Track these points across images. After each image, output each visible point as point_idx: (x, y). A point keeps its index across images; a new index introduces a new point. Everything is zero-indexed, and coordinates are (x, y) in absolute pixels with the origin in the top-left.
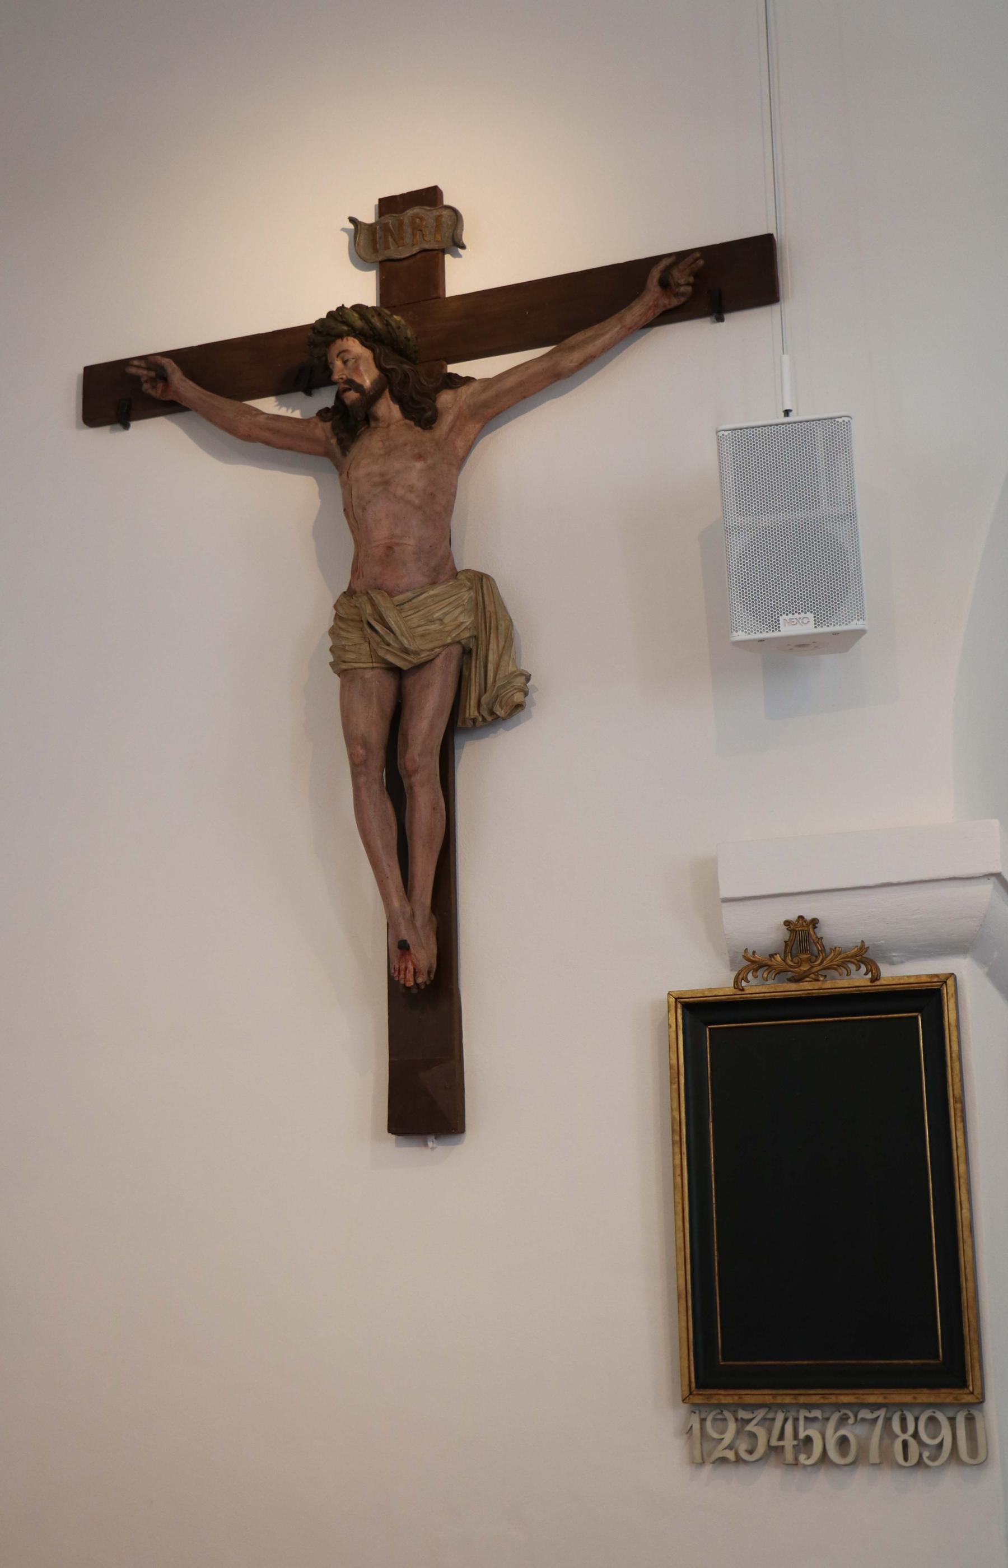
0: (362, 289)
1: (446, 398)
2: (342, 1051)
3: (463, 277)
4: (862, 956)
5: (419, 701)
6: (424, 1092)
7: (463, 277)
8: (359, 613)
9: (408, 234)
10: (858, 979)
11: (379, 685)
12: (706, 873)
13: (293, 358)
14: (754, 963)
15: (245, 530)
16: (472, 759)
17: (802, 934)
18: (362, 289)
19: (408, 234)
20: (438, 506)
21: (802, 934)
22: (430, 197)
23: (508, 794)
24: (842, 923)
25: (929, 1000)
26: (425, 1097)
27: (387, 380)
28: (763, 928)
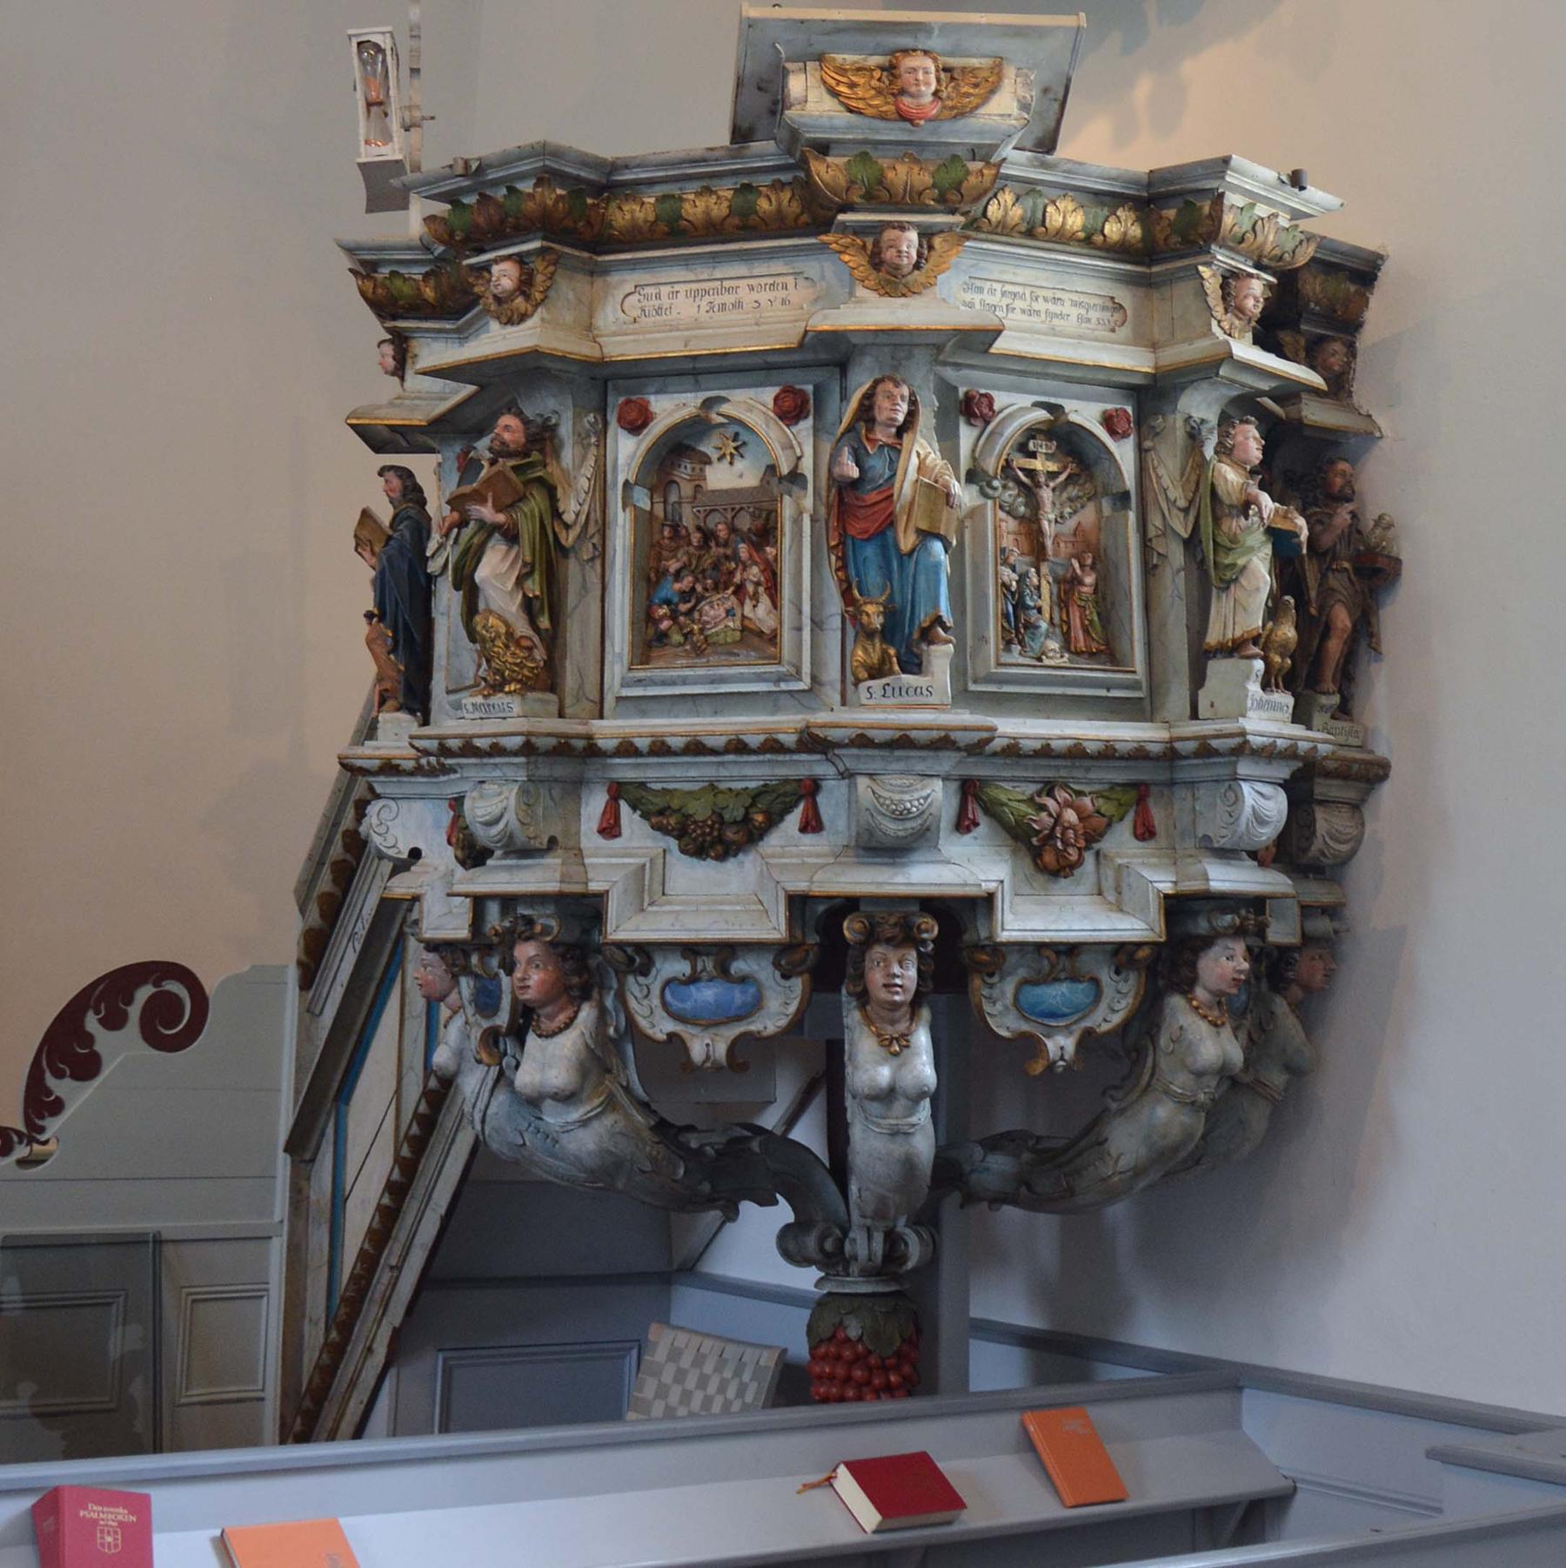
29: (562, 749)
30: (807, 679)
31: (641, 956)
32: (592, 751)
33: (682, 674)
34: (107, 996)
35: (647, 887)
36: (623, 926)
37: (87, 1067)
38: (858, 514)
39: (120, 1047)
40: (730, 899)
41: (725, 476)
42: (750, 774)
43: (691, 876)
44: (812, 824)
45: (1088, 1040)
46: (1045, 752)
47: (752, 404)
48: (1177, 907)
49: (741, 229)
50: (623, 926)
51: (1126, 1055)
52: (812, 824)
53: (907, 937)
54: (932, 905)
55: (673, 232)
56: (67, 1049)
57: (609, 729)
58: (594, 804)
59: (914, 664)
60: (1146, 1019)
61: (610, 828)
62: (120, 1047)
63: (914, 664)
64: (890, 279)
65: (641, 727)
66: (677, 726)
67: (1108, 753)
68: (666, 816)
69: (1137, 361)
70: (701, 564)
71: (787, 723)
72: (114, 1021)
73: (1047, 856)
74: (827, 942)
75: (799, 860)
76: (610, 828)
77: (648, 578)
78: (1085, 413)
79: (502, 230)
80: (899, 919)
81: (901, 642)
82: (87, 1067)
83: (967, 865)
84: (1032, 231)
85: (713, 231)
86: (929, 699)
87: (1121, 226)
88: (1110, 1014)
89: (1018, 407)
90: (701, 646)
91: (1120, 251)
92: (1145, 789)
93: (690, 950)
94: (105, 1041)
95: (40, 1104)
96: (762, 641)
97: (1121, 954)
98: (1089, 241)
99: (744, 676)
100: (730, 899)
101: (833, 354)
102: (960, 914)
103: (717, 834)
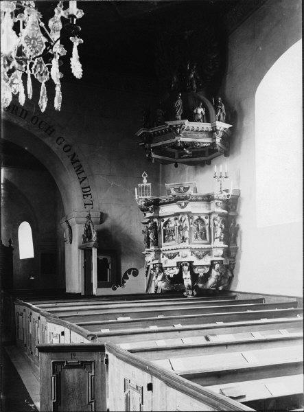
31: (166, 268)
33: (167, 244)
35: (166, 262)
37: (128, 278)
39: (130, 276)
40: (173, 262)
41: (170, 226)
43: (169, 261)
44: (179, 256)
47: (172, 219)
48: (212, 262)
50: (164, 266)
51: (207, 276)
52: (179, 256)
53: (186, 265)
54: (188, 262)
60: (210, 271)
61: (163, 257)
62: (130, 276)
64: (183, 208)
68: (167, 256)
69: (208, 212)
72: (130, 274)
73: (199, 257)
74: (180, 265)
75: (178, 259)
76: (163, 257)
78: (203, 217)
79: (150, 205)
82: (128, 278)
86: (186, 244)
87: (207, 198)
88: (207, 270)
89: (196, 217)
90: (169, 241)
92: (209, 252)
94: (129, 276)
96: (173, 240)
97: (207, 266)
98: (203, 200)
99: (173, 243)
100: (173, 262)
101: (178, 214)
102: (191, 263)
103: (171, 258)
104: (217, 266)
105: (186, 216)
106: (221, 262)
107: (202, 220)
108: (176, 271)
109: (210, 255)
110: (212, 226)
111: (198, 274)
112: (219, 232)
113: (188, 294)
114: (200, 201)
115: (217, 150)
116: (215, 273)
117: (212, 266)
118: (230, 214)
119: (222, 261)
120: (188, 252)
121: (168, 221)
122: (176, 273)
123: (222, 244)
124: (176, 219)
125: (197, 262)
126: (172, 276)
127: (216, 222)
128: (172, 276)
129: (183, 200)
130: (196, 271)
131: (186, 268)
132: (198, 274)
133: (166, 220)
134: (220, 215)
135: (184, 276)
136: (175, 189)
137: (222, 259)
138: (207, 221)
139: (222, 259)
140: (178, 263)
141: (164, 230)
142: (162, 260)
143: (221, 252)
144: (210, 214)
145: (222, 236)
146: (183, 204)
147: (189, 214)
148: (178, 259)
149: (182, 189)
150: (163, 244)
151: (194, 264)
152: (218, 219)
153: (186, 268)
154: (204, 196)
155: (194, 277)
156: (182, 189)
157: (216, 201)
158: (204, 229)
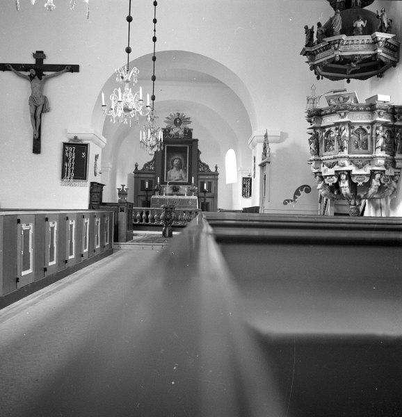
0: (33, 61)
1: (43, 77)
2: (30, 145)
3: (46, 62)
4: (81, 140)
5: (39, 109)
6: (37, 149)
7: (46, 62)
8: (33, 99)
9: (39, 56)
10: (80, 143)
11: (34, 107)
12: (66, 130)
13: (26, 67)
14: (71, 140)
15: (17, 89)
16: (43, 115)
17: (76, 138)
18: (33, 61)
19: (39, 56)
20: (41, 89)
21: (76, 138)
22: (42, 52)
23: (48, 120)
24: (79, 137)
25: (86, 145)
26: (37, 149)
27: (36, 74)
28: (72, 137)
29: (318, 160)
30: (186, 146)
31: (326, 176)
32: (320, 160)
33: (328, 153)
34: (301, 188)
36: (323, 174)
37: (299, 195)
38: (339, 138)
39: (303, 193)
40: (331, 172)
41: (332, 136)
42: (333, 161)
43: (329, 170)
45: (363, 183)
46: (358, 158)
47: (333, 129)
49: (331, 113)
53: (344, 174)
54: (347, 171)
55: (326, 114)
56: (297, 193)
57: (322, 158)
58: (322, 165)
59: (343, 151)
60: (370, 181)
63: (343, 151)
64: (343, 117)
65: (326, 157)
66: (329, 157)
67: (365, 158)
68: (327, 165)
69: (370, 121)
70: (329, 143)
71: (332, 157)
73: (359, 167)
74: (338, 174)
75: (337, 168)
77: (326, 145)
80: (343, 172)
81: (342, 149)
82: (299, 195)
83: (348, 167)
84: (358, 110)
85: (329, 114)
86: (345, 153)
88: (367, 180)
89: (357, 127)
91: (369, 111)
92: (370, 161)
93: (329, 176)
94: (301, 192)
95: (295, 198)
97: (367, 175)
98: (365, 110)
99: (332, 153)
100: (331, 172)
101: (337, 124)
102: (349, 172)
103: (331, 167)
104: (378, 176)
105: (347, 127)
106: (382, 172)
107: (363, 129)
108: (335, 180)
109: (370, 165)
110: (374, 136)
111: (357, 183)
112: (381, 141)
113: (350, 204)
114: (361, 111)
115: (382, 64)
116: (375, 183)
117: (373, 174)
118: (395, 124)
119: (384, 171)
120: (346, 162)
121: (330, 131)
122: (335, 182)
123: (383, 154)
124: (336, 129)
125: (355, 172)
126: (330, 184)
127: (378, 131)
128: (330, 184)
129: (343, 110)
130: (354, 180)
131: (344, 177)
132: (357, 183)
133: (327, 130)
134: (385, 125)
135: (342, 185)
136: (335, 100)
137: (384, 169)
138: (369, 131)
139: (384, 169)
140: (336, 172)
141: (326, 140)
142: (322, 169)
143: (382, 162)
144: (372, 124)
145: (385, 146)
146: (343, 114)
147: (351, 125)
148: (337, 168)
149: (341, 99)
150: (324, 154)
151: (354, 173)
152: (381, 128)
153: (344, 177)
154: (367, 106)
155: (353, 186)
156: (341, 99)
157: (378, 110)
158: (367, 140)
